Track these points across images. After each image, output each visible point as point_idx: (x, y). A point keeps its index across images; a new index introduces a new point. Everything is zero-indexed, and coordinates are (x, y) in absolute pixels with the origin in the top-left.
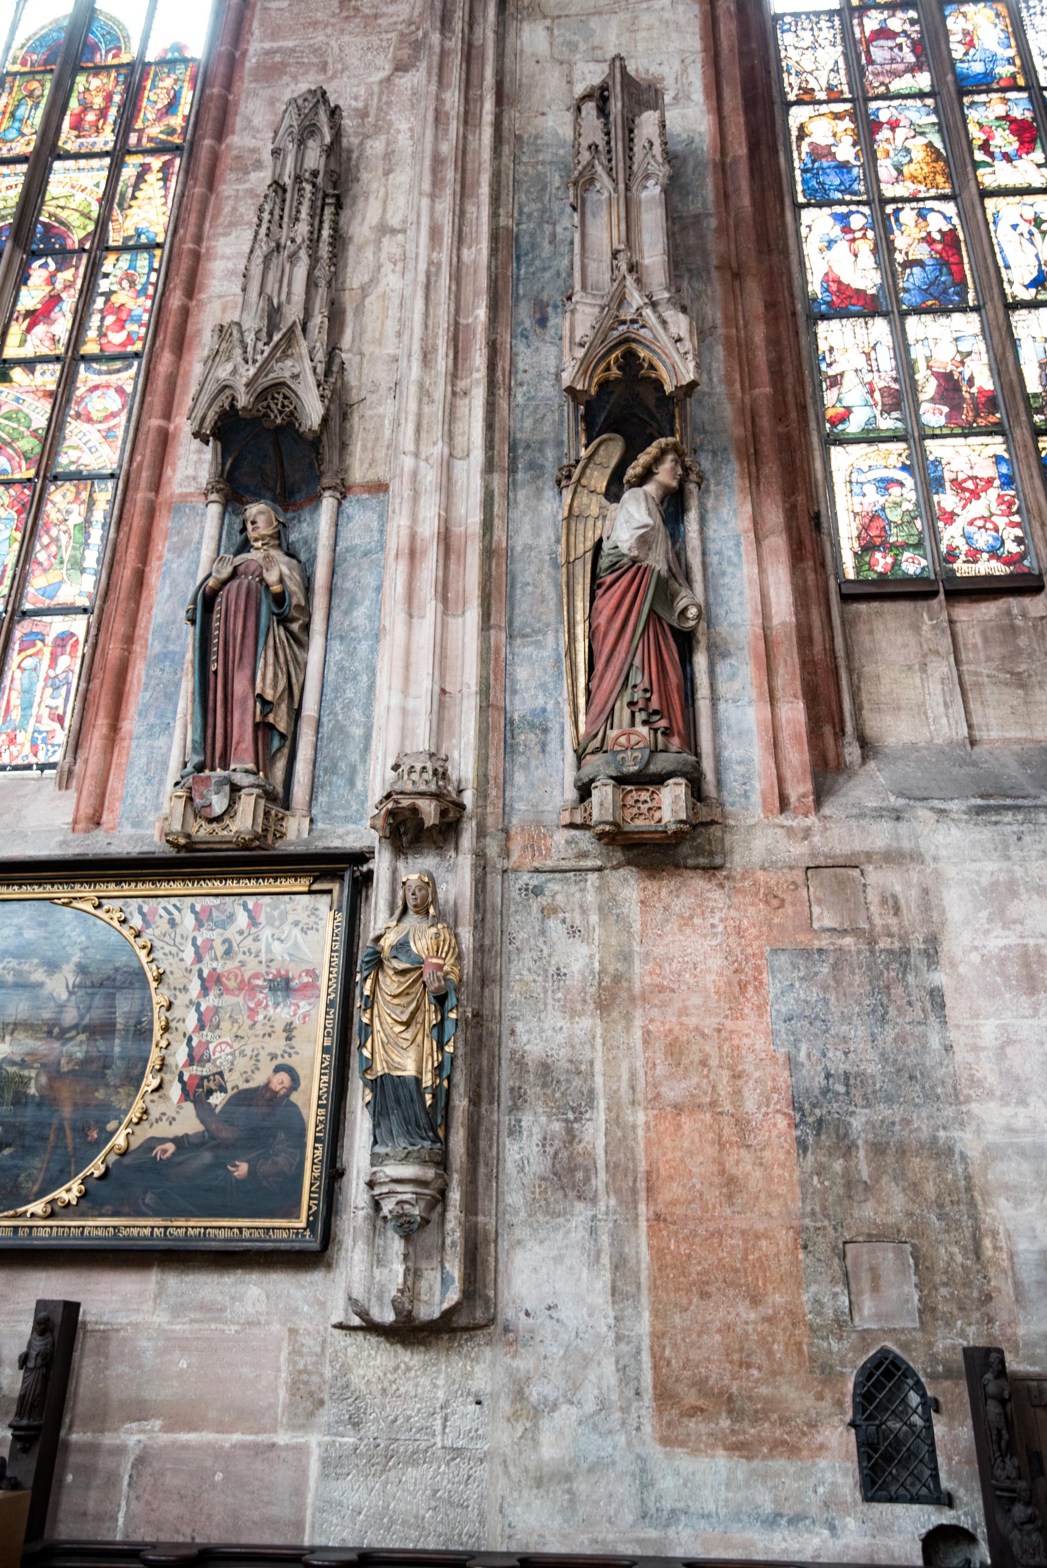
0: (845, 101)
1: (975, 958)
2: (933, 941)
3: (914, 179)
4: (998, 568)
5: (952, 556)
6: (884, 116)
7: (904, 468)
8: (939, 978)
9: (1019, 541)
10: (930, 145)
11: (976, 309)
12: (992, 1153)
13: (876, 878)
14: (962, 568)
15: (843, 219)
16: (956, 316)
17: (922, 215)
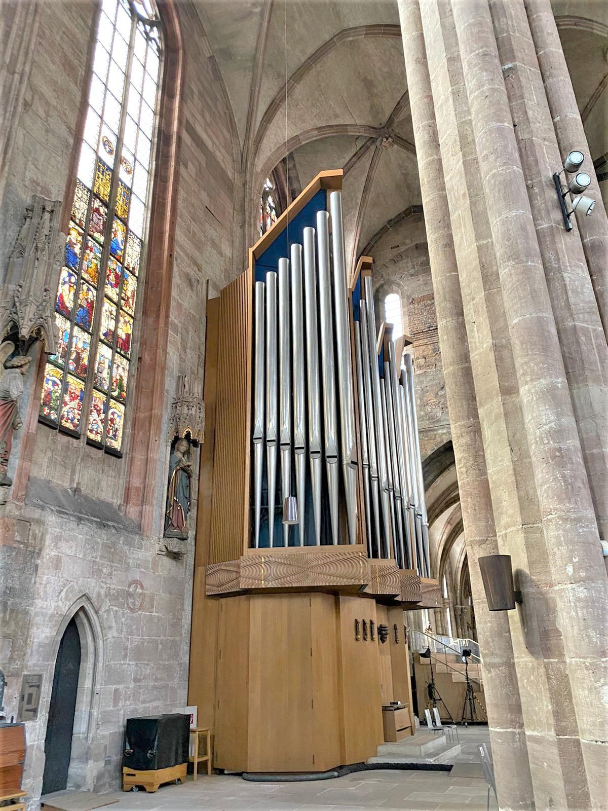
0: (83, 229)
1: (48, 556)
2: (40, 550)
3: (90, 274)
4: (72, 428)
5: (62, 417)
6: (90, 244)
7: (61, 380)
8: (39, 562)
9: (78, 420)
10: (97, 265)
11: (91, 334)
12: (36, 614)
13: (34, 527)
14: (64, 423)
15: (70, 275)
16: (86, 333)
17: (89, 290)
